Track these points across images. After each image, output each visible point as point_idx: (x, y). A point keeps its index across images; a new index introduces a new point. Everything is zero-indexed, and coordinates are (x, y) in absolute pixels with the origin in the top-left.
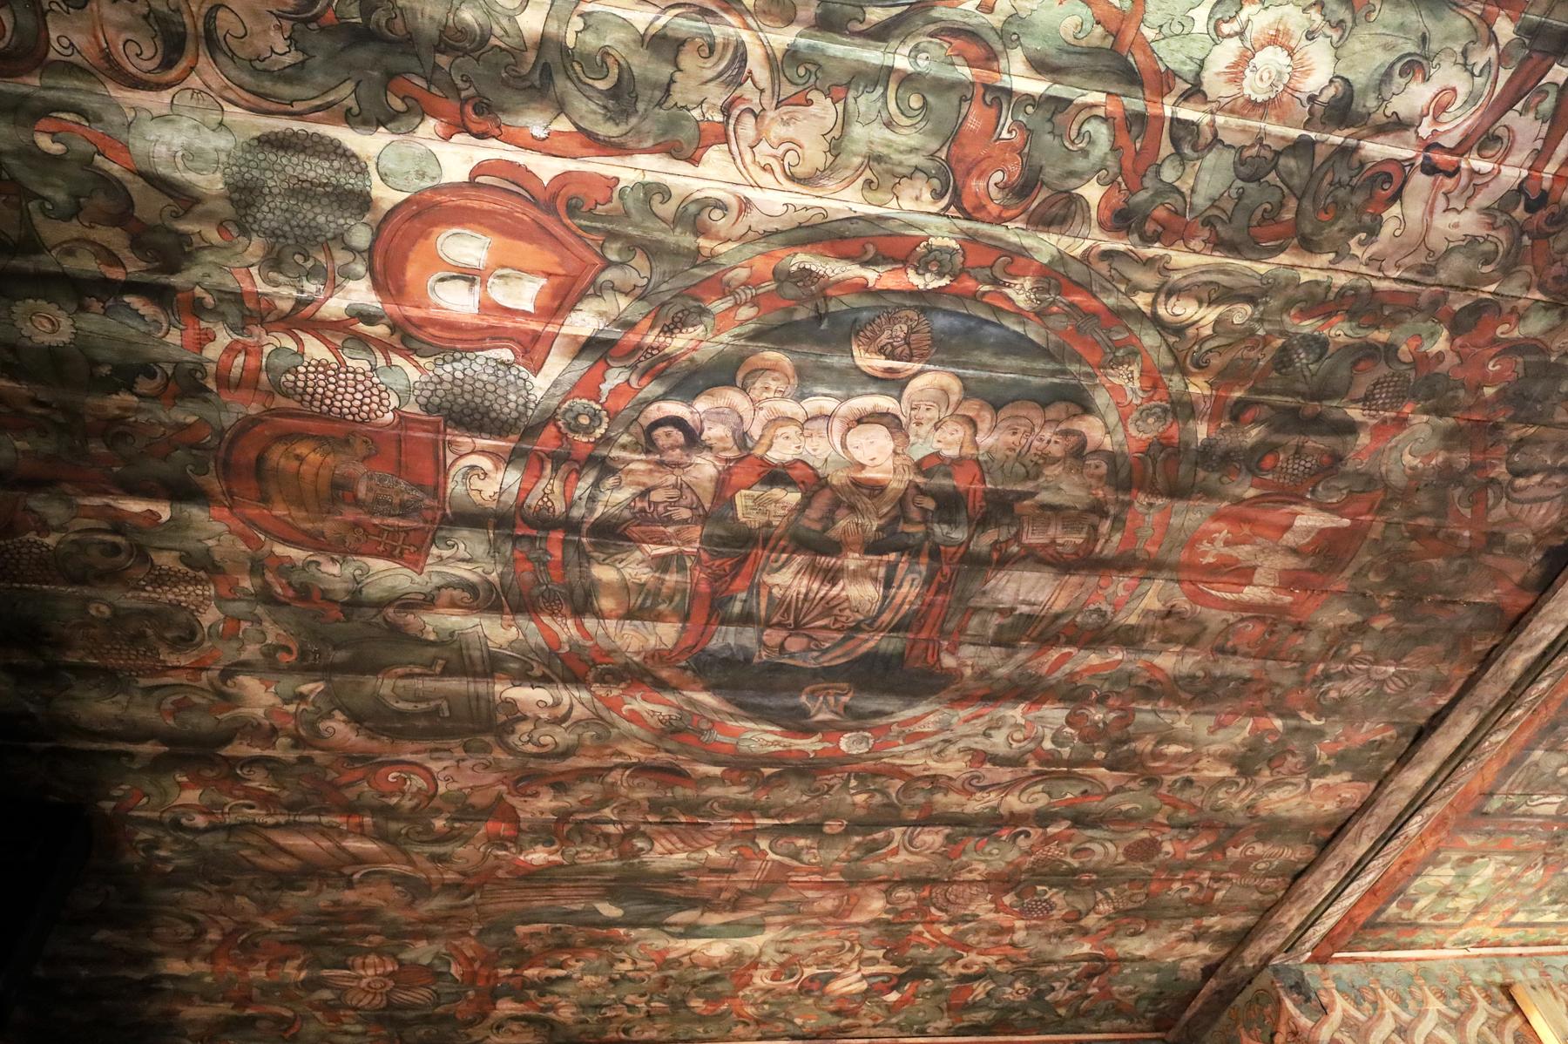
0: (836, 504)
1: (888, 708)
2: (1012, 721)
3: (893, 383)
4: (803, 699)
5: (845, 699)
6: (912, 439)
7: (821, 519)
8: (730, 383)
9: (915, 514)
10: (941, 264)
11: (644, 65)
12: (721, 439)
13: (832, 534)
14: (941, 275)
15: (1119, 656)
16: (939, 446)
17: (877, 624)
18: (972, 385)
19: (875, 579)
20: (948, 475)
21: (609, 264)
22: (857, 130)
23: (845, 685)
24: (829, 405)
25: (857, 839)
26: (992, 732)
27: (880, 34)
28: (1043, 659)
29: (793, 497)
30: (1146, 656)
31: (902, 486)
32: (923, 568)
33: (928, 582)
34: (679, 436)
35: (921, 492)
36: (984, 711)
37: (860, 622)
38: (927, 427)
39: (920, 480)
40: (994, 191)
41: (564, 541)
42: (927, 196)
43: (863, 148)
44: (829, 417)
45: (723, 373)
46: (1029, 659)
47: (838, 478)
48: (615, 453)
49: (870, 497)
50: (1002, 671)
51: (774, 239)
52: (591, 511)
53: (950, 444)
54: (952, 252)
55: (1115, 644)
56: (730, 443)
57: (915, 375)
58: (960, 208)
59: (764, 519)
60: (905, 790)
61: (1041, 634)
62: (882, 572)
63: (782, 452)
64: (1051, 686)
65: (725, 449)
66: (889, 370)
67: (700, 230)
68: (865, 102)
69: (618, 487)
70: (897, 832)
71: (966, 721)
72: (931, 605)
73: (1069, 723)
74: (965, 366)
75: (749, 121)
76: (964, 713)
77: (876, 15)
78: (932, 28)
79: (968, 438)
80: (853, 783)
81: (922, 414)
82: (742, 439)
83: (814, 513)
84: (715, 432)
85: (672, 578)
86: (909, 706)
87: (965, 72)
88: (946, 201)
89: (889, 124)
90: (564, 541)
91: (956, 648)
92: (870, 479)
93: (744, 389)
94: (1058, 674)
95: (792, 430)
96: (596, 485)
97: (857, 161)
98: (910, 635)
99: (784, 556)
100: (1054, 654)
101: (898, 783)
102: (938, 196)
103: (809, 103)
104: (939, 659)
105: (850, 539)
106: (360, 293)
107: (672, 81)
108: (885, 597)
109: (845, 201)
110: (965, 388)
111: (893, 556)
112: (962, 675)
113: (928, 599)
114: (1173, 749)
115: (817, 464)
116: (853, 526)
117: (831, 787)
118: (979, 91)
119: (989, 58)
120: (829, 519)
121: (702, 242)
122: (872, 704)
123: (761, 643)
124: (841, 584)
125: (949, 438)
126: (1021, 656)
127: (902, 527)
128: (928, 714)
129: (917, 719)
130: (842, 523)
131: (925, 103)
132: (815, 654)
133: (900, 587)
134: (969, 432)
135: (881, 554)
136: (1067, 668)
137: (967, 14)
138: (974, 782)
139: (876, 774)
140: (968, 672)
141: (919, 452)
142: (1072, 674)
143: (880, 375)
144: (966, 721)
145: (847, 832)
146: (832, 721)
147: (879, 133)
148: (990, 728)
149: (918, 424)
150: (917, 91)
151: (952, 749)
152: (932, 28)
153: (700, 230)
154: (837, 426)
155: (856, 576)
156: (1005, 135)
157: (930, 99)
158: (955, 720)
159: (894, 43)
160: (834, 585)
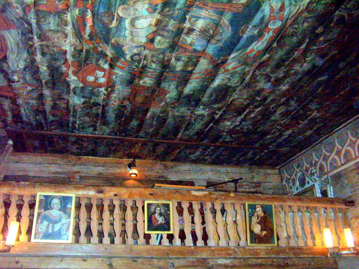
0: (163, 30)
1: (261, 16)
3: (120, 20)
5: (250, 27)
6: (140, 15)
7: (168, 33)
8: (121, 49)
9: (171, 13)
10: (84, 11)
11: (48, 57)
12: (137, 50)
13: (174, 30)
14: (87, 11)
16: (144, 9)
18: (121, 3)
19: (196, 21)
20: (156, 5)
21: (91, 63)
22: (52, 28)
24: (127, 33)
27: (30, 24)
29: (159, 38)
31: (159, 15)
32: (195, 9)
33: (201, 8)
34: (137, 56)
35: (162, 10)
38: (137, 12)
39: (158, 11)
40: (60, 3)
41: (167, 73)
42: (66, 15)
43: (56, 27)
44: (131, 33)
45: (119, 49)
47: (154, 29)
48: (141, 65)
49: (162, 22)
51: (82, 41)
52: (158, 69)
53: (143, 7)
54: (80, 10)
56: (140, 49)
57: (118, 15)
58: (68, 8)
59: (165, 43)
62: (194, 19)
63: (144, 40)
65: (141, 49)
66: (117, 20)
67: (81, 51)
68: (46, 27)
69: (151, 66)
72: (211, 7)
74: (115, 5)
75: (55, 44)
77: (26, 26)
78: (25, 17)
79: (141, 2)
81: (132, 13)
82: (136, 47)
83: (166, 34)
84: (135, 51)
85: (183, 59)
87: (33, 10)
88: (67, 12)
89: (49, 23)
90: (167, 73)
92: (155, 23)
93: (123, 46)
95: (136, 39)
96: (149, 68)
97: (59, 28)
99: (181, 39)
102: (65, 13)
103: (48, 36)
105: (177, 26)
106: (103, 89)
107: (50, 54)
108: (203, 18)
109: (69, 29)
110: (123, 4)
111: (188, 17)
113: (209, 8)
115: (148, 33)
116: (172, 26)
118: (36, 8)
119: (28, 6)
120: (168, 31)
121: (84, 51)
122: (256, 20)
123: (215, 44)
124: (196, 28)
125: (141, 7)
127: (175, 15)
130: (170, 28)
131: (42, 18)
133: (201, 15)
134: (139, 2)
135: (186, 19)
137: (20, 11)
141: (146, 13)
143: (118, 23)
146: (260, 29)
147: (51, 25)
149: (135, 14)
150: (40, 20)
152: (25, 17)
153: (81, 51)
154: (135, 30)
155: (192, 24)
156: (45, 2)
157: (41, 17)
159: (31, 22)
160: (195, 30)
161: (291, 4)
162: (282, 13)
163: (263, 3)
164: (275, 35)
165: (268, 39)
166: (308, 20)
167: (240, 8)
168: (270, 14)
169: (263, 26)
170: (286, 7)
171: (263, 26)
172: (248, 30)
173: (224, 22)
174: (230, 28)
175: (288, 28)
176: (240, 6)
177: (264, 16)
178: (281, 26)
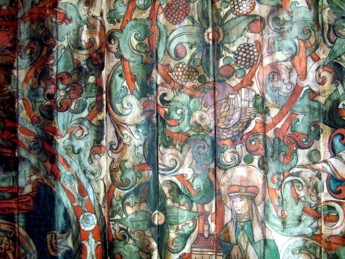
2: (67, 142)
4: (59, 255)
15: (21, 102)
17: (11, 230)
23: (48, 237)
25: (169, 202)
26: (76, 149)
28: (24, 142)
30: (20, 87)
36: (60, 159)
37: (9, 238)
46: (24, 148)
50: (33, 160)
55: (14, 108)
60: (123, 185)
61: (9, 148)
64: (41, 129)
70: (161, 180)
71: (68, 166)
73: (68, 108)
76: (62, 169)
80: (118, 217)
86: (60, 201)
91: (21, 188)
94: (33, 129)
98: (16, 212)
100: (21, 136)
101: (117, 191)
104: (28, 195)
112: (36, 180)
114: (85, 38)
117: (121, 229)
122: (60, 221)
126: (23, 153)
128: (64, 188)
129: (69, 194)
132: (28, 256)
136: (29, 126)
138: (114, 147)
139: (110, 205)
140: (34, 177)
142: (33, 122)
144: (68, 166)
145: (163, 209)
146: (73, 237)
148: (73, 152)
151: (91, 168)
158: (68, 173)
161: (89, 181)
162: (87, 197)
163: (54, 186)
164: (99, 243)
165: (94, 253)
166: (127, 201)
167: (29, 201)
168: (72, 206)
169: (74, 230)
170: (85, 186)
171: (74, 230)
172: (59, 241)
173: (19, 233)
174: (31, 242)
175: (109, 224)
176: (29, 198)
177: (66, 210)
178: (98, 222)
